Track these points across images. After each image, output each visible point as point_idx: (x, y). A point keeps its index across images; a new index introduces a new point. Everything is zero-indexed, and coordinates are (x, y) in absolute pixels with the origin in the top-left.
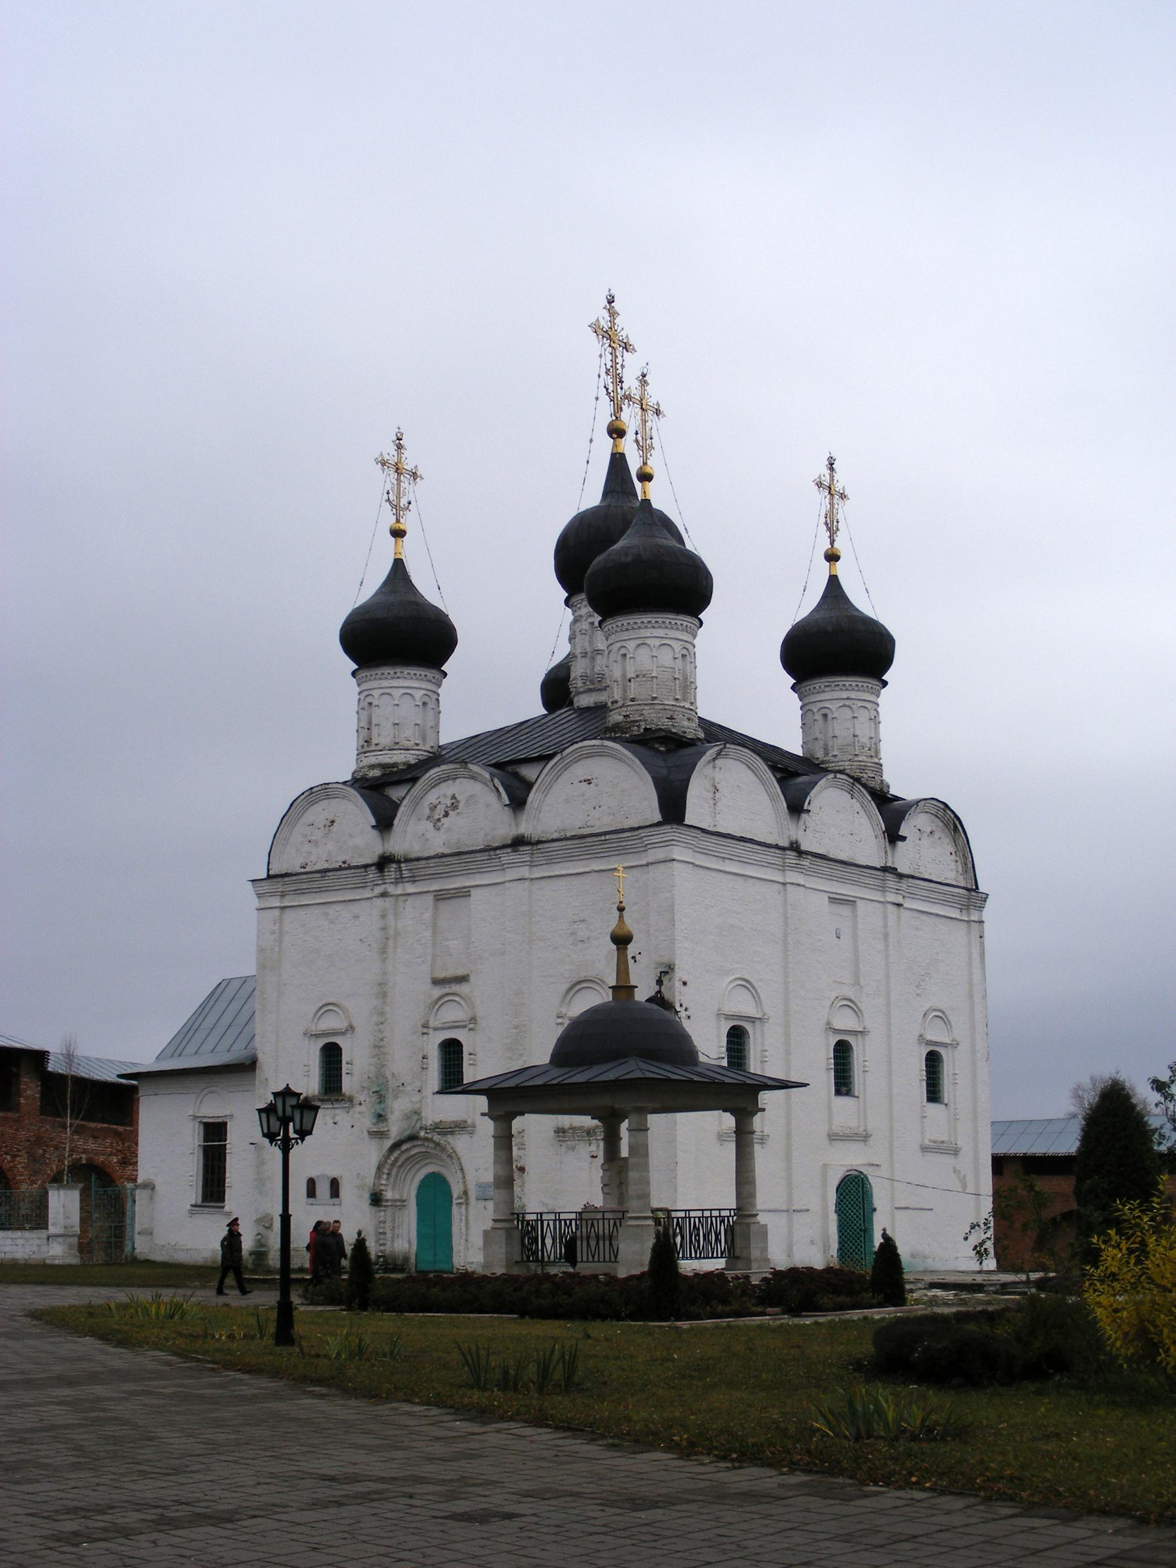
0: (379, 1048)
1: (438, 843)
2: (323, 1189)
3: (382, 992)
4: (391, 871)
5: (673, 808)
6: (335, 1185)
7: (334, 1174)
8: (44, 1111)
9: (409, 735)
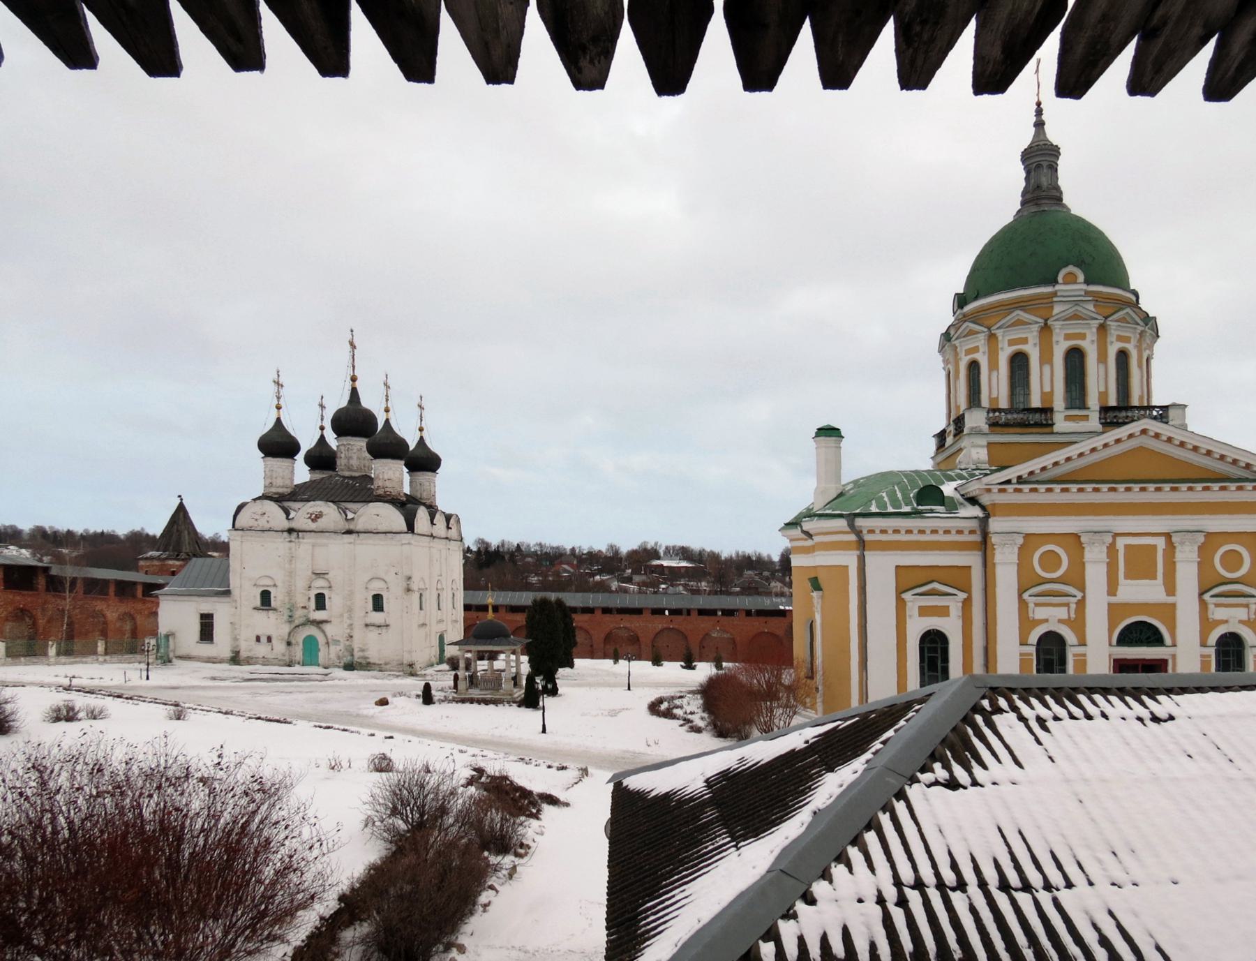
0: (290, 593)
1: (313, 526)
2: (264, 639)
3: (291, 574)
4: (295, 534)
5: (411, 528)
6: (269, 639)
7: (269, 633)
8: (48, 590)
9: (288, 482)
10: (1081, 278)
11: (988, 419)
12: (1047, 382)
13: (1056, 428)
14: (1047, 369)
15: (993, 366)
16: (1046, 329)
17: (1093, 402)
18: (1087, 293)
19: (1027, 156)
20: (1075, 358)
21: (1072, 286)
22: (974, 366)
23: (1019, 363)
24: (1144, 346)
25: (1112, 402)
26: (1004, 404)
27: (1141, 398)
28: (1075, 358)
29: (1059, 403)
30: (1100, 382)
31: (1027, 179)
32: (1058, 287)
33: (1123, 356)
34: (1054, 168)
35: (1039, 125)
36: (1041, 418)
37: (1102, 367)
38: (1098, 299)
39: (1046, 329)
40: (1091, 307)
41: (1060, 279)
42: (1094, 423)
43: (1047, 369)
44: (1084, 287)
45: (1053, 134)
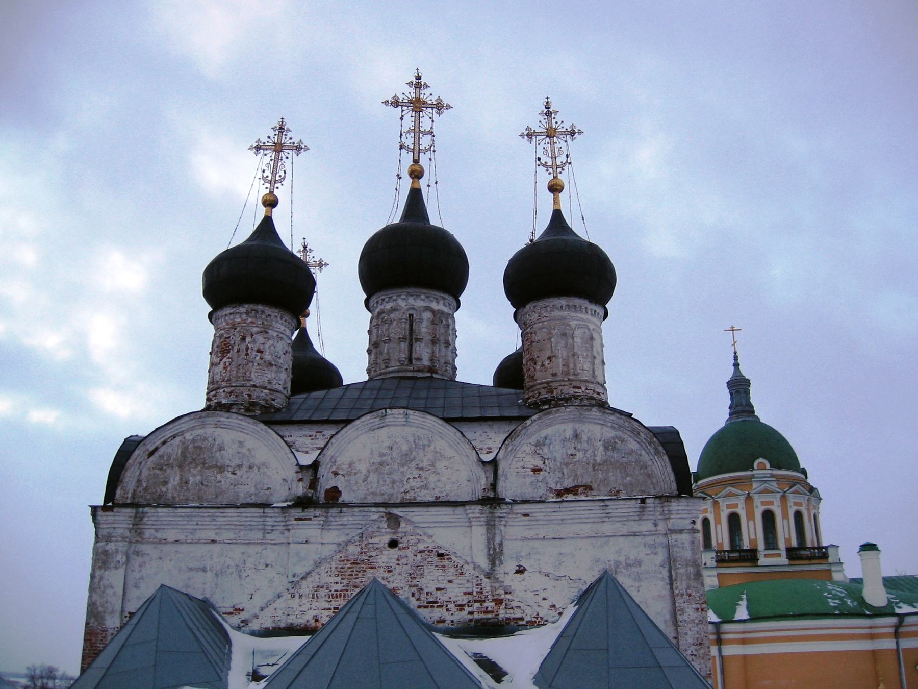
10: (768, 466)
11: (717, 556)
12: (752, 533)
13: (760, 563)
14: (751, 523)
15: (718, 521)
16: (749, 498)
17: (782, 545)
18: (772, 476)
19: (730, 384)
20: (768, 518)
21: (762, 468)
22: (706, 522)
23: (734, 520)
24: (811, 507)
25: (794, 543)
26: (727, 547)
27: (812, 541)
28: (768, 518)
29: (761, 546)
30: (785, 532)
31: (732, 399)
32: (754, 472)
33: (798, 516)
34: (747, 393)
35: (736, 365)
36: (751, 556)
37: (786, 522)
38: (779, 478)
39: (749, 498)
40: (775, 484)
41: (755, 467)
42: (783, 560)
43: (751, 523)
44: (770, 472)
45: (745, 372)
